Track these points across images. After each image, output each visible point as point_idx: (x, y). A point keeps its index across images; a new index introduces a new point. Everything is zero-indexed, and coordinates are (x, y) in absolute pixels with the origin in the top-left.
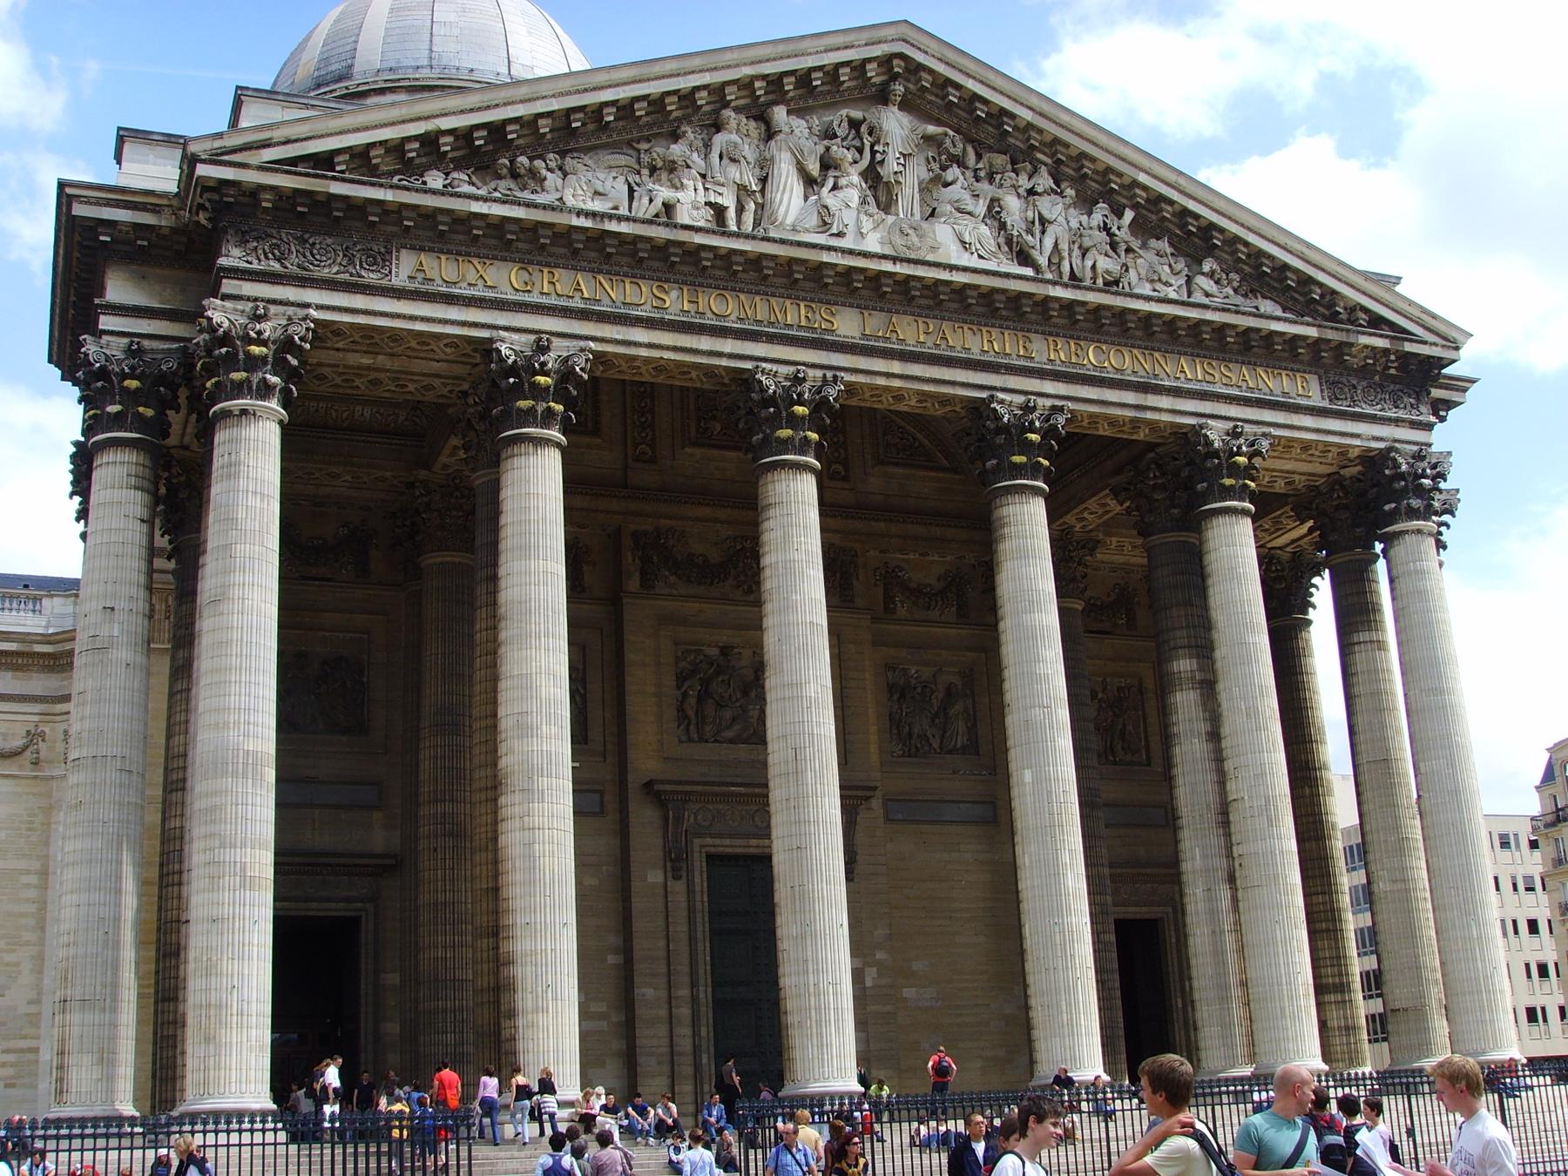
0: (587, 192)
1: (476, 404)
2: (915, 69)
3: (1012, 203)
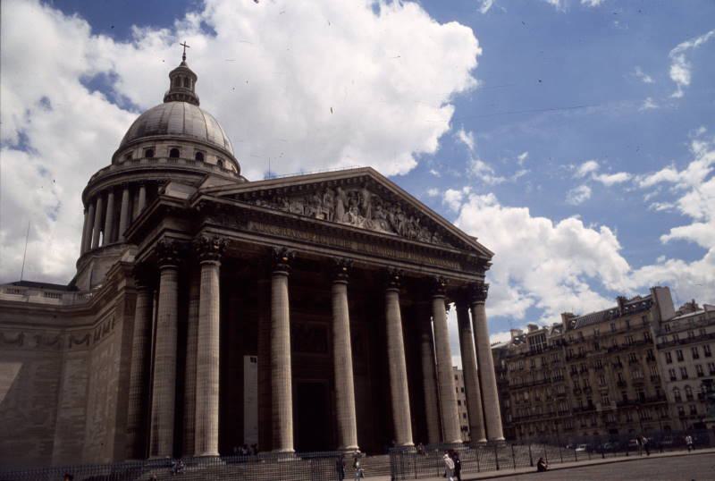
0: (295, 208)
1: (267, 263)
2: (371, 179)
3: (392, 216)
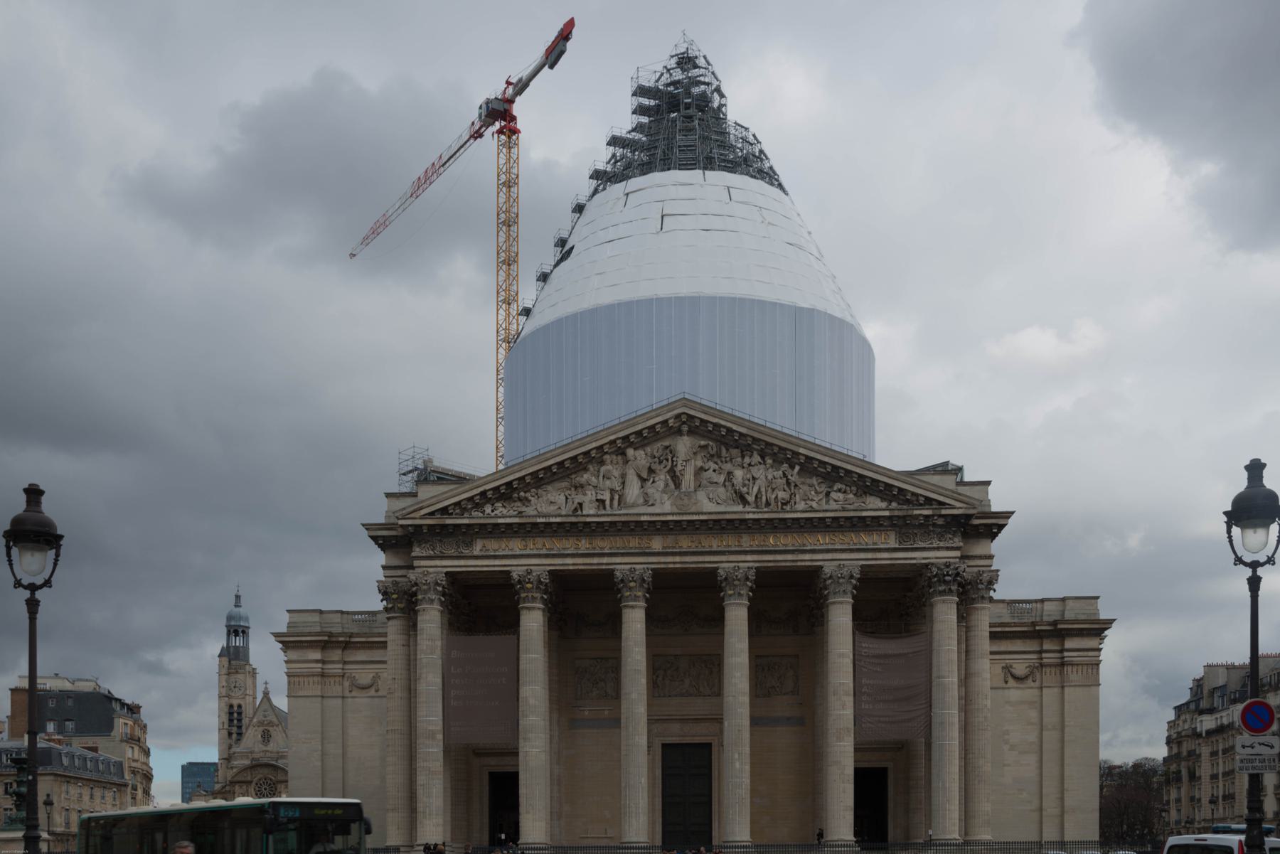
3: (739, 474)
